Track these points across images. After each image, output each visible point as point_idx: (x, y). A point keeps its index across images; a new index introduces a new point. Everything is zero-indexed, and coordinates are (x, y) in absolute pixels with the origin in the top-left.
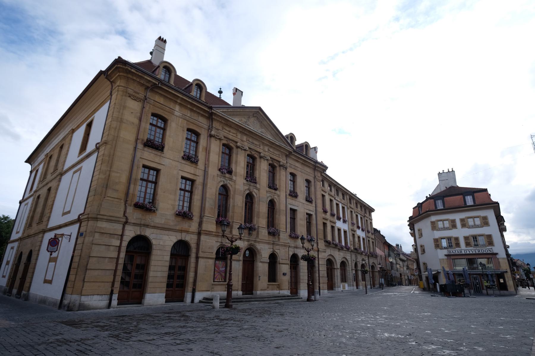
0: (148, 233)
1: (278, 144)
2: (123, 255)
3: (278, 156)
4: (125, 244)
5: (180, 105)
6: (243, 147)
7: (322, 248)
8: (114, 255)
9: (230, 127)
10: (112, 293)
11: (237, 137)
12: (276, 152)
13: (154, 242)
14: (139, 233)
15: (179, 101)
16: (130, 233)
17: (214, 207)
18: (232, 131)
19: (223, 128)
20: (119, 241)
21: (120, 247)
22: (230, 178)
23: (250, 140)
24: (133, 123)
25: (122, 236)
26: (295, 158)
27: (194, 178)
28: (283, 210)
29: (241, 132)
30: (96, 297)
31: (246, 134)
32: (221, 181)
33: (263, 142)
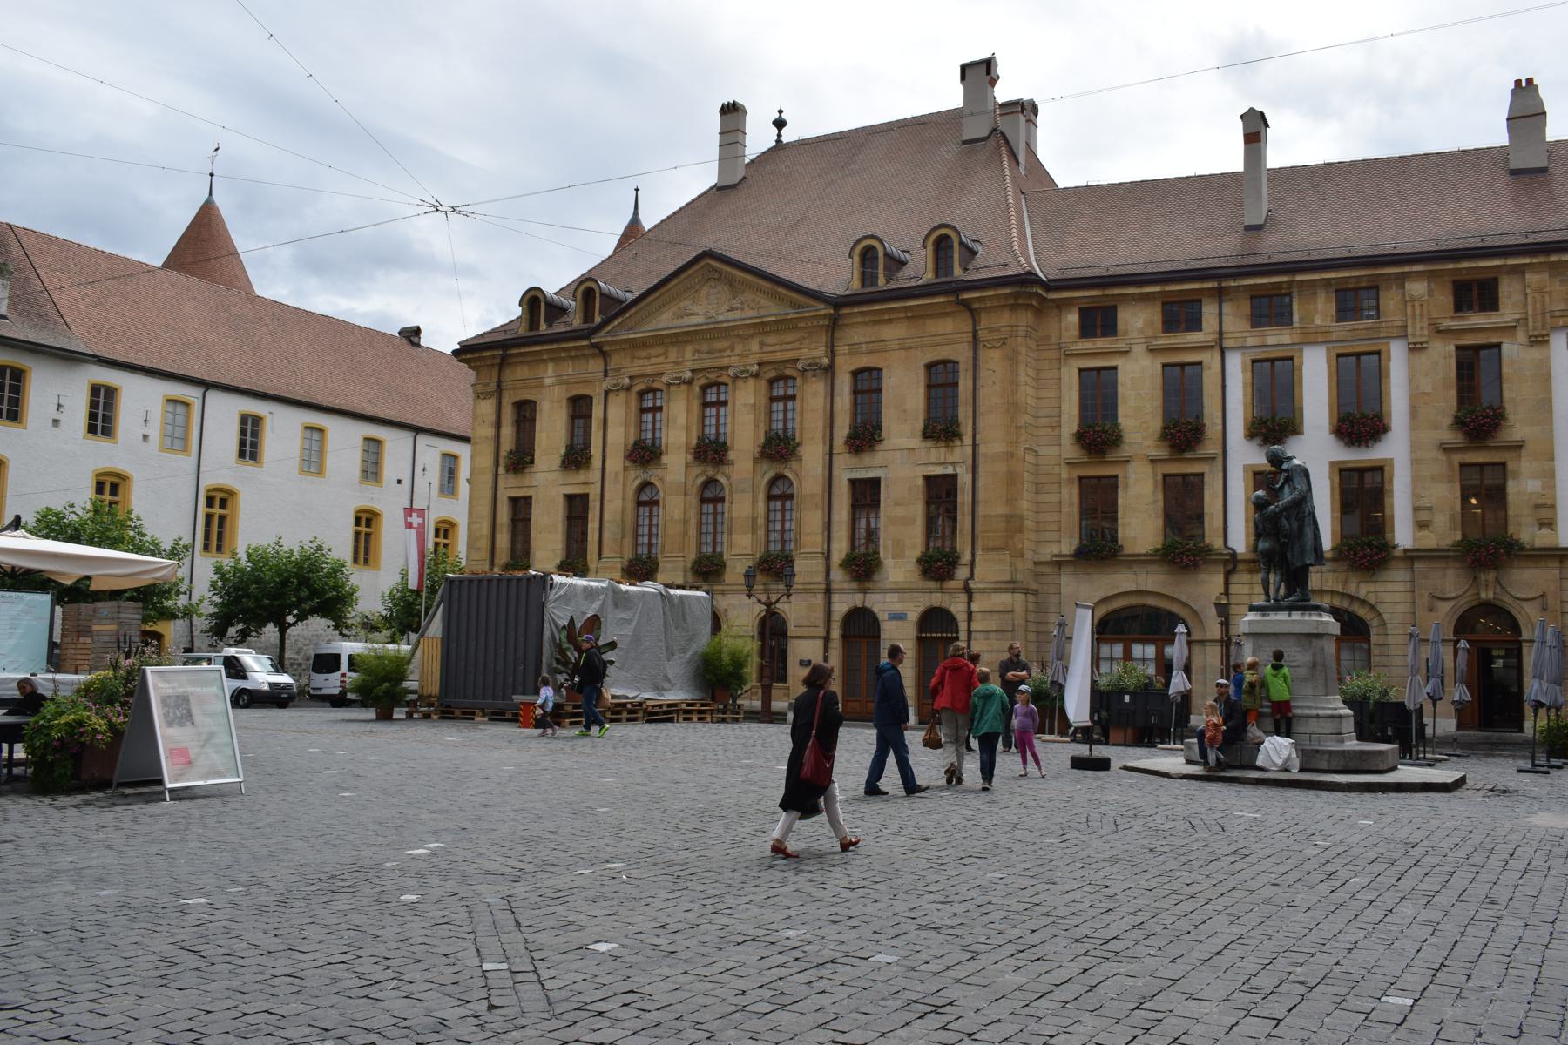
1: (774, 319)
5: (552, 360)
6: (680, 378)
7: (993, 579)
12: (790, 337)
15: (545, 357)
17: (620, 537)
18: (654, 351)
19: (633, 358)
23: (705, 347)
24: (487, 438)
26: (867, 320)
27: (586, 491)
28: (813, 495)
31: (686, 342)
32: (636, 478)
33: (738, 336)
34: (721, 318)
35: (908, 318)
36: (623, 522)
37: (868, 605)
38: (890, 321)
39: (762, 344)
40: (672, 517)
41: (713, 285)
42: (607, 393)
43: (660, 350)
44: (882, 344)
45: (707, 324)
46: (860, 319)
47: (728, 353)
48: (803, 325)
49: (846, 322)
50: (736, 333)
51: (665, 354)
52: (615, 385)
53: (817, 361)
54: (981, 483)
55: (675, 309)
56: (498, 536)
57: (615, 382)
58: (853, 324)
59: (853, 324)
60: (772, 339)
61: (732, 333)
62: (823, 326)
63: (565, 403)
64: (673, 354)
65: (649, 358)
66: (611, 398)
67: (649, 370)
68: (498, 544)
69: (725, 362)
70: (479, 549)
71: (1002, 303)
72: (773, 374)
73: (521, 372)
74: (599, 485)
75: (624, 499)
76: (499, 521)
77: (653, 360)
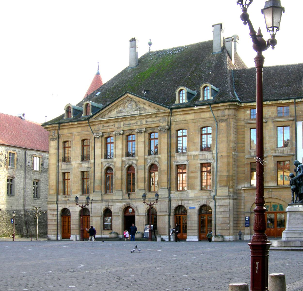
0: (68, 207)
1: (150, 113)
2: (59, 218)
3: (158, 122)
4: (59, 213)
6: (119, 133)
8: (56, 218)
9: (107, 123)
10: (57, 234)
11: (115, 127)
13: (71, 211)
14: (63, 207)
16: (60, 208)
17: (100, 185)
20: (56, 212)
21: (57, 214)
22: (111, 161)
23: (127, 122)
24: (54, 153)
25: (57, 209)
28: (164, 170)
29: (116, 122)
30: (52, 235)
34: (133, 113)
35: (195, 113)
36: (101, 180)
37: (183, 205)
38: (189, 114)
39: (146, 121)
40: (118, 178)
41: (130, 102)
42: (95, 138)
43: (112, 124)
44: (187, 121)
45: (128, 115)
46: (179, 113)
47: (135, 124)
48: (160, 115)
49: (174, 114)
50: (138, 118)
51: (114, 125)
52: (97, 136)
53: (165, 127)
54: (219, 165)
55: (117, 110)
56: (59, 185)
57: (97, 134)
58: (177, 115)
59: (177, 115)
60: (150, 120)
61: (136, 118)
62: (167, 116)
63: (80, 142)
64: (117, 125)
65: (109, 126)
66: (96, 139)
67: (109, 130)
68: (60, 188)
69: (134, 127)
70: (53, 189)
71: (225, 108)
72: (150, 131)
73: (66, 131)
74: (93, 168)
75: (101, 172)
76: (59, 180)
77: (110, 127)
